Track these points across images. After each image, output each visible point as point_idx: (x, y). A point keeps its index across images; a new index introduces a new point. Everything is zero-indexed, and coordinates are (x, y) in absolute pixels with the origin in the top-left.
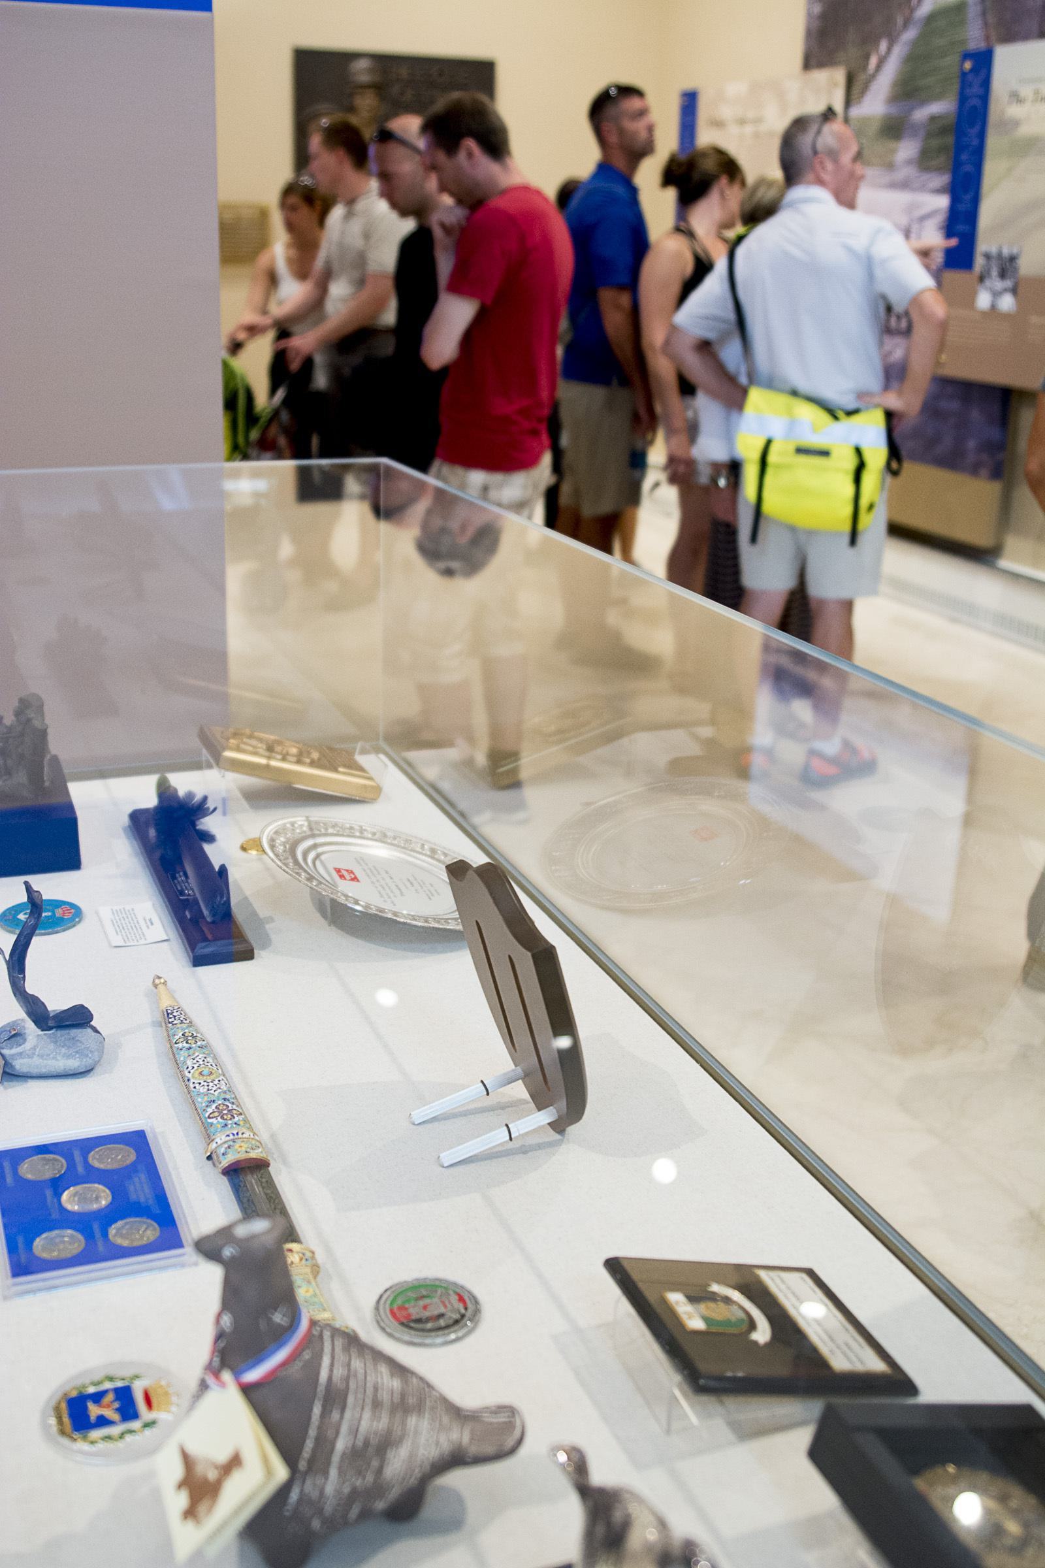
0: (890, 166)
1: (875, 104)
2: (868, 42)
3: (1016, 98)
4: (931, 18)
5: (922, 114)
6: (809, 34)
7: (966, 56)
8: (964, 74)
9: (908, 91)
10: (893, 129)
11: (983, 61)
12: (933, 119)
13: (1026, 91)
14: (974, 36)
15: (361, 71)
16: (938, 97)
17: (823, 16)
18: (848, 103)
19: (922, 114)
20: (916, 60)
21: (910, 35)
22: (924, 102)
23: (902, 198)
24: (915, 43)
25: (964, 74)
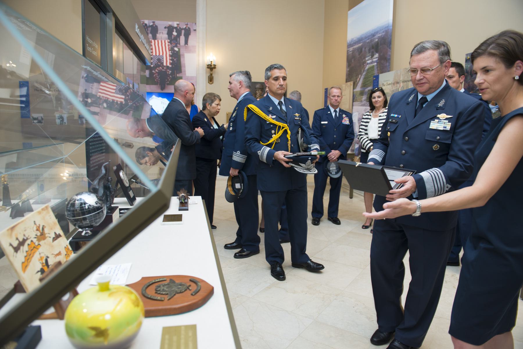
0: (361, 101)
1: (358, 89)
2: (357, 76)
3: (383, 85)
4: (368, 69)
5: (367, 90)
6: (347, 75)
7: (374, 77)
8: (374, 80)
9: (364, 85)
10: (362, 93)
11: (377, 77)
12: (369, 90)
13: (385, 83)
14: (375, 72)
15: (258, 86)
16: (370, 86)
17: (349, 71)
18: (354, 89)
19: (367, 90)
20: (365, 78)
21: (364, 73)
22: (367, 87)
23: (364, 108)
24: (365, 75)
25: (374, 80)
